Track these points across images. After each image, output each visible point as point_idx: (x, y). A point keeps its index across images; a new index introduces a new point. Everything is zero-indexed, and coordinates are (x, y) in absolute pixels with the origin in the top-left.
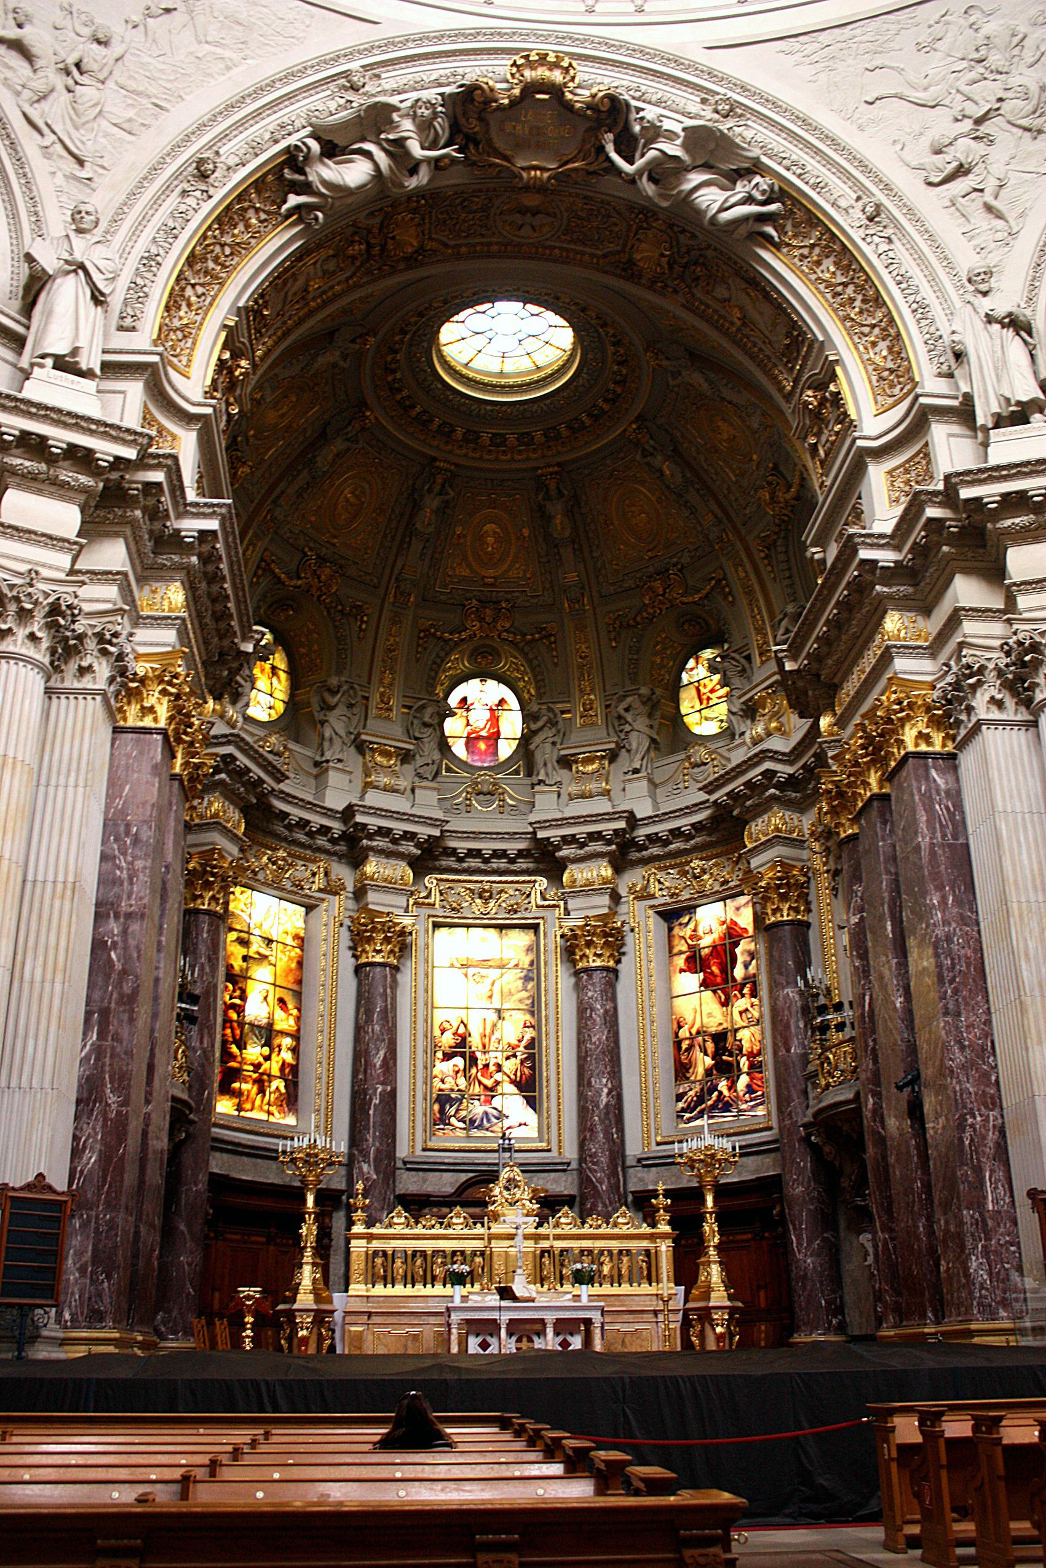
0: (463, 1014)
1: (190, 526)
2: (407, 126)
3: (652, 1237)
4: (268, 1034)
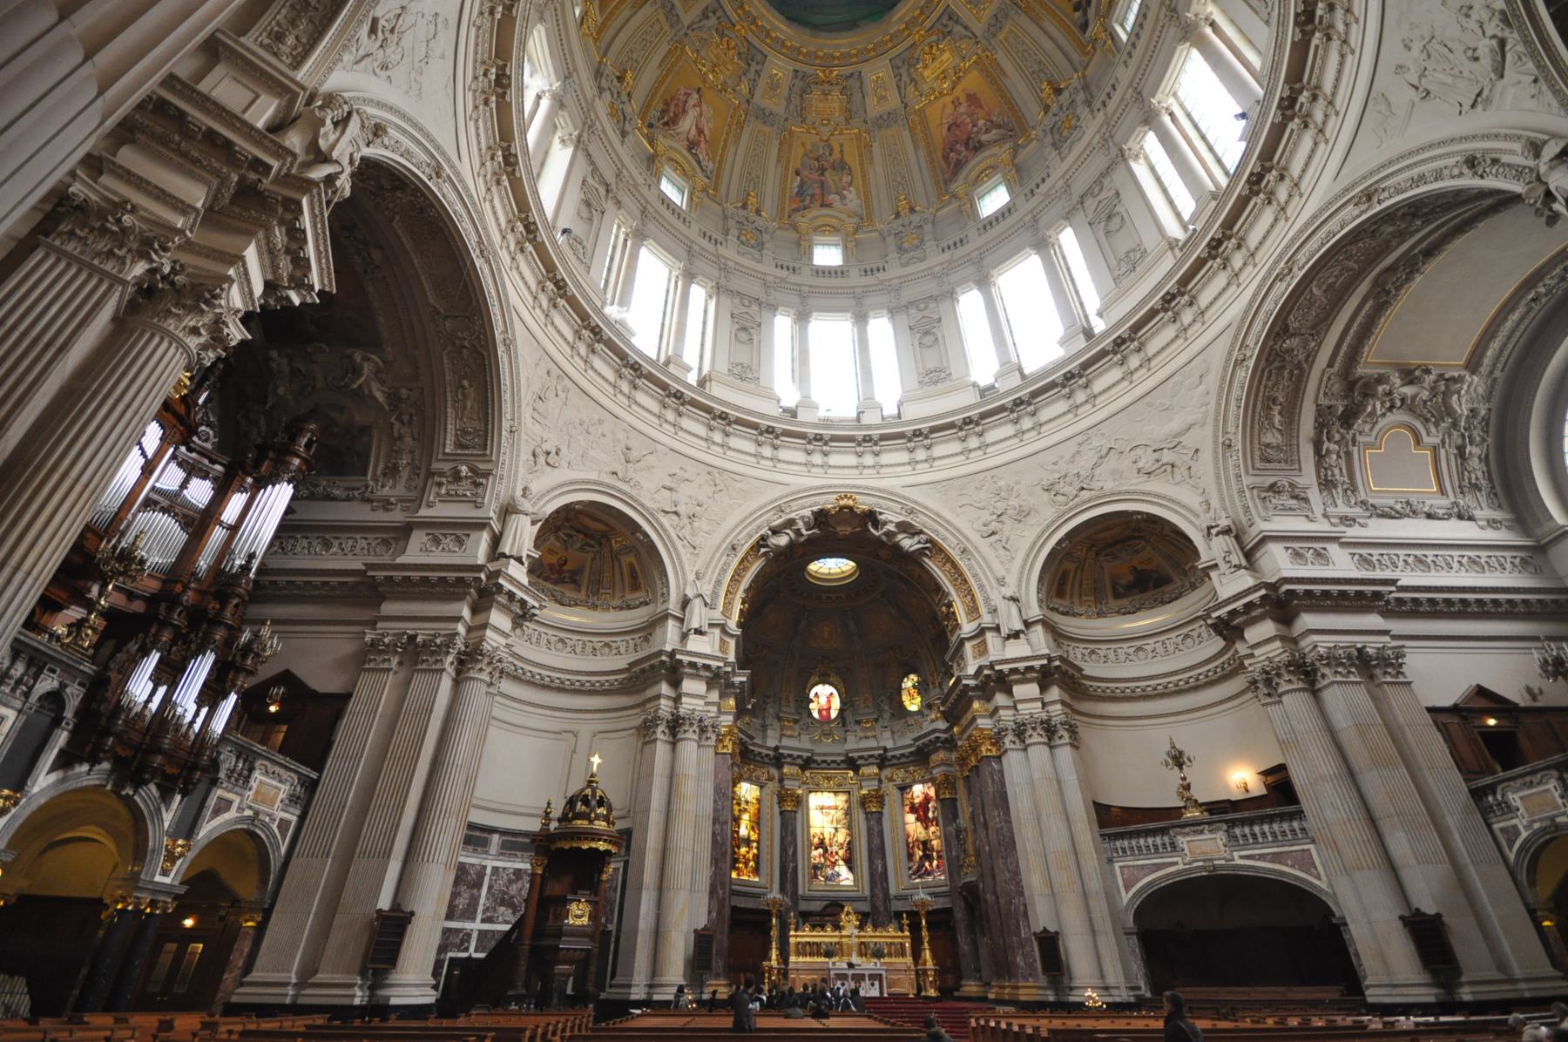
2: (800, 524)
3: (902, 937)
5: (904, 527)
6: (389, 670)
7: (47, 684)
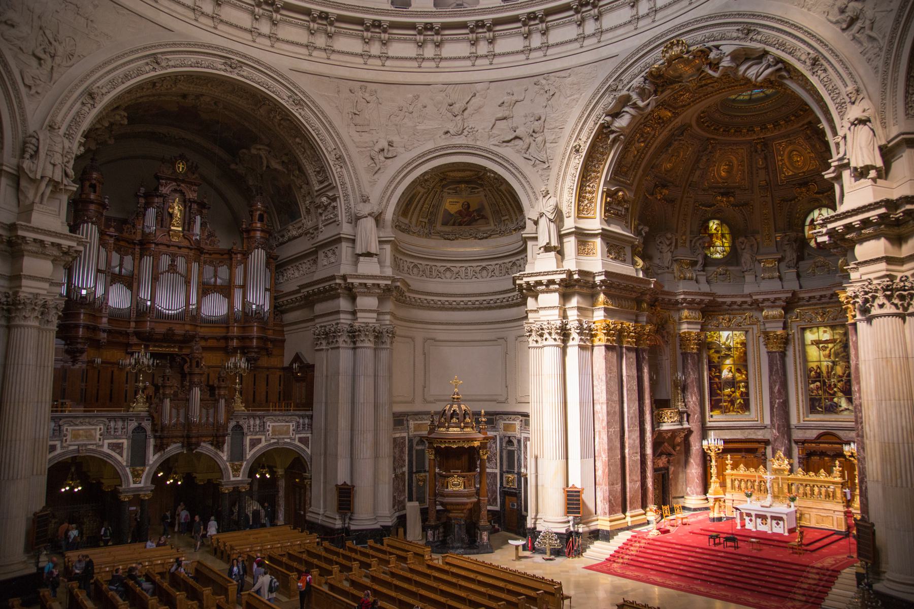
0: (818, 364)
1: (598, 279)
2: (634, 97)
4: (732, 383)
5: (742, 56)
6: (322, 350)
7: (133, 424)
